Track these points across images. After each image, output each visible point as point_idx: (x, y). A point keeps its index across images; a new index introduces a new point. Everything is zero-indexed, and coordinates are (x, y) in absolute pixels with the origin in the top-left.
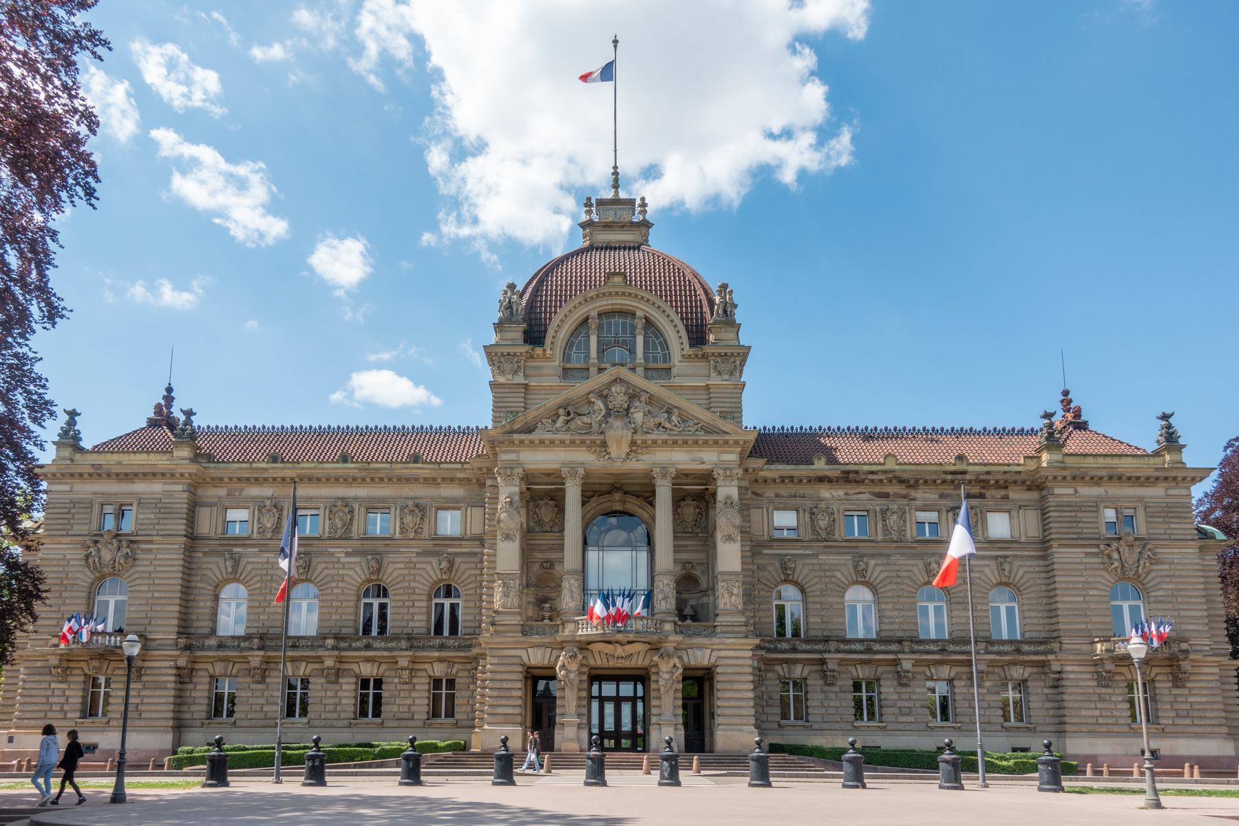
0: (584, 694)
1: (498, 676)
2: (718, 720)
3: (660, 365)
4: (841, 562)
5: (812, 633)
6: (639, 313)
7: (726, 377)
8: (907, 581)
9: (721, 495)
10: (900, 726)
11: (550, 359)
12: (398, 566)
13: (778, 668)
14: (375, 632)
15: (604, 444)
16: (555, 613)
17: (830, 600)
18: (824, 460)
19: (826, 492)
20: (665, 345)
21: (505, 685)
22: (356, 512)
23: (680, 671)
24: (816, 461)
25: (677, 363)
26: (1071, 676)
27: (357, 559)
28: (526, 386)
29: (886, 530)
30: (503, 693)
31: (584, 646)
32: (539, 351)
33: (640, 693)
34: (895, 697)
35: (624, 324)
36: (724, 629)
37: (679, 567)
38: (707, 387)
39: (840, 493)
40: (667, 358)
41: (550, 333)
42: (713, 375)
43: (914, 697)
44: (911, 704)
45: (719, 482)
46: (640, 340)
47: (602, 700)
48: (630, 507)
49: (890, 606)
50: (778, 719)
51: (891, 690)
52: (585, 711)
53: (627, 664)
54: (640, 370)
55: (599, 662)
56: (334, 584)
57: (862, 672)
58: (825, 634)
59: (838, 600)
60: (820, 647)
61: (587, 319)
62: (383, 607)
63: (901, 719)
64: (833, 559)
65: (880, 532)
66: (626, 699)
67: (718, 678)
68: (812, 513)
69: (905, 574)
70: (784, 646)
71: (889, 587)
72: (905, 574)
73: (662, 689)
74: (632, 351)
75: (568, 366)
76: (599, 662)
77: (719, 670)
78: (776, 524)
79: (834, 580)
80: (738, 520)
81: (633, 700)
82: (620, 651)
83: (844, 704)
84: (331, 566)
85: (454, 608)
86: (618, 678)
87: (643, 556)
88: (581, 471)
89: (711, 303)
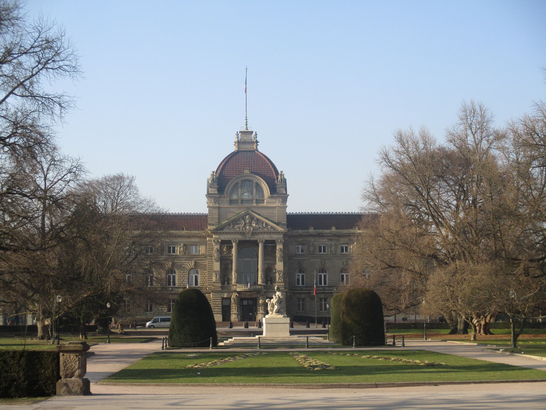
3: (261, 198)
6: (254, 181)
11: (227, 197)
13: (297, 295)
16: (229, 280)
18: (312, 228)
19: (312, 239)
20: (262, 191)
28: (219, 208)
29: (331, 251)
31: (238, 292)
32: (223, 196)
35: (249, 184)
37: (266, 266)
40: (263, 196)
41: (226, 189)
46: (254, 190)
54: (254, 201)
55: (243, 296)
57: (322, 296)
60: (309, 289)
61: (238, 183)
70: (299, 288)
74: (252, 194)
82: (248, 294)
89: (278, 178)
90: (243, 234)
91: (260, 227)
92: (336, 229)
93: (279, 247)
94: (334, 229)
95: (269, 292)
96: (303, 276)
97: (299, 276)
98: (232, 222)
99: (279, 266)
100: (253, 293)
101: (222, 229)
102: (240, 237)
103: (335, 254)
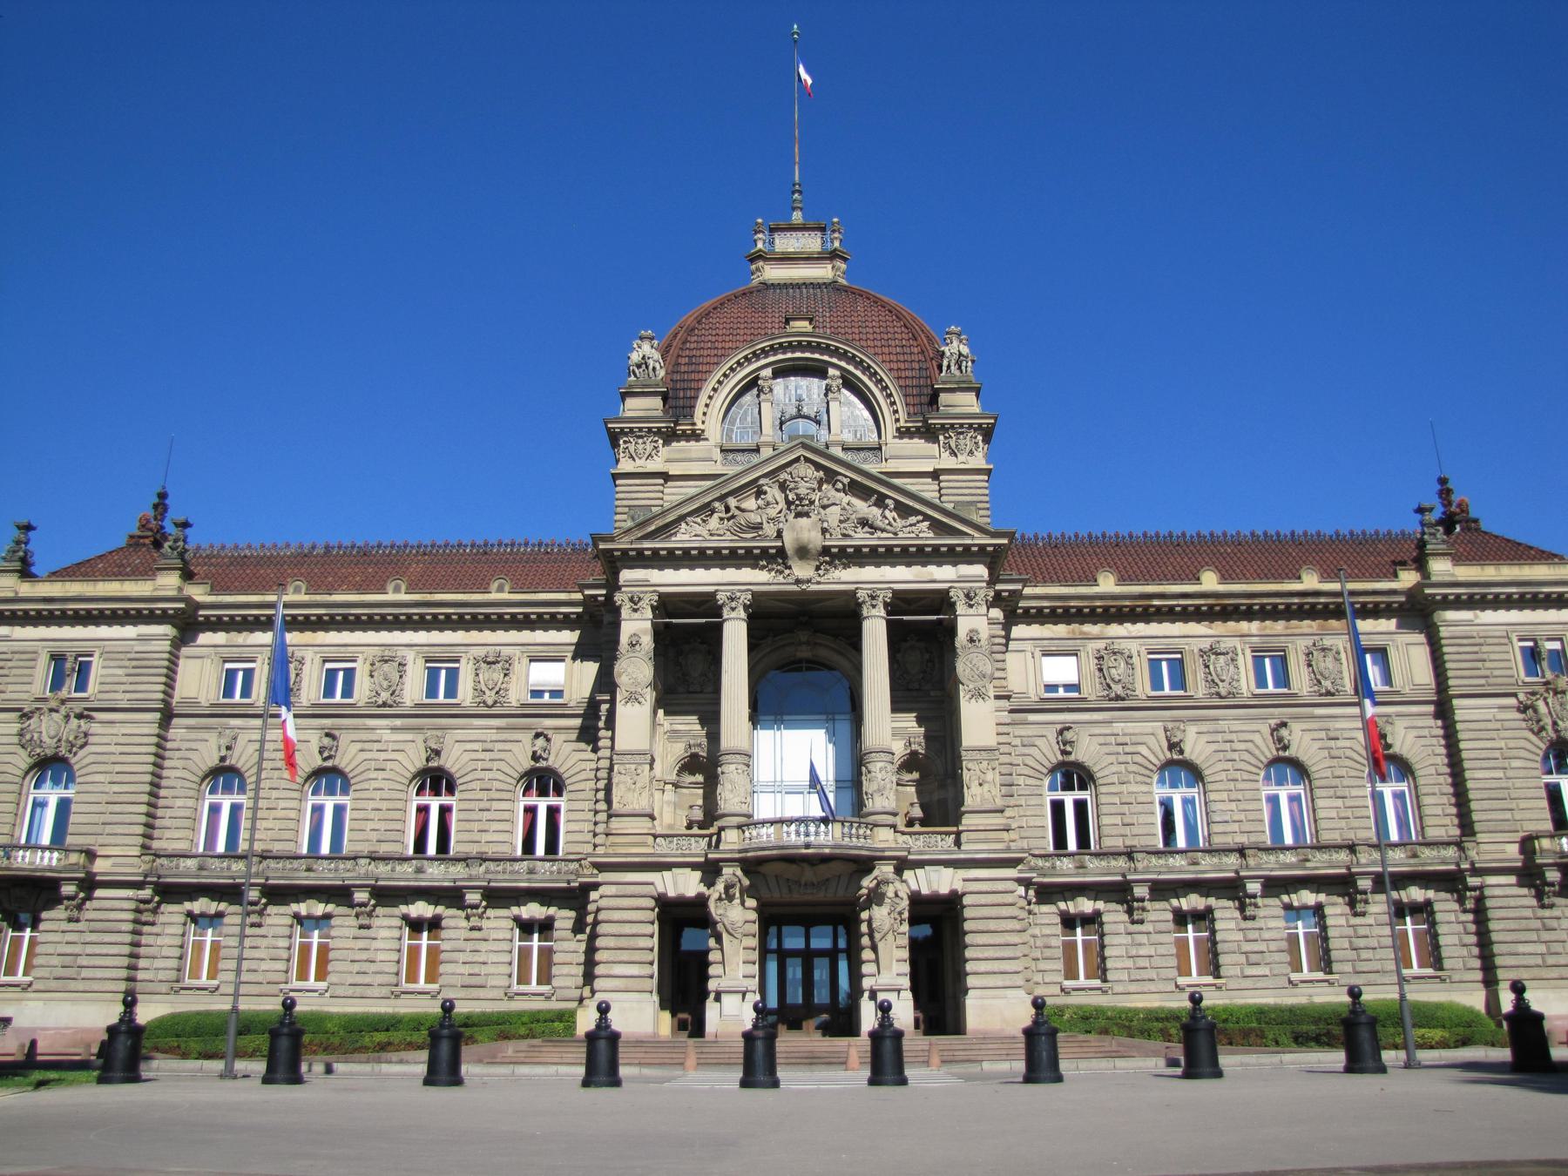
0: (754, 942)
1: (616, 915)
2: (971, 981)
4: (1148, 734)
5: (1108, 843)
6: (831, 372)
7: (961, 458)
8: (1246, 756)
9: (964, 626)
10: (1248, 983)
12: (469, 746)
14: (432, 848)
15: (781, 552)
17: (1134, 788)
21: (628, 929)
22: (409, 668)
23: (905, 903)
24: (1101, 579)
25: (890, 439)
26: (1497, 892)
27: (409, 736)
28: (666, 477)
30: (623, 942)
33: (842, 944)
34: (1240, 936)
36: (973, 835)
38: (935, 475)
39: (1140, 628)
41: (703, 399)
42: (946, 455)
43: (1266, 935)
44: (1262, 947)
45: (961, 608)
47: (783, 955)
48: (823, 653)
49: (1224, 796)
50: (1060, 978)
51: (1232, 925)
52: (755, 969)
53: (821, 896)
55: (776, 894)
56: (373, 775)
58: (1128, 843)
59: (1144, 788)
62: (445, 811)
63: (1250, 971)
64: (1131, 727)
65: (1202, 685)
66: (821, 953)
67: (967, 913)
68: (1100, 658)
69: (1242, 746)
71: (1220, 766)
72: (1242, 746)
73: (877, 936)
75: (728, 446)
76: (776, 895)
77: (966, 900)
78: (1050, 678)
79: (1138, 759)
80: (988, 668)
81: (832, 955)
82: (809, 874)
83: (1162, 950)
84: (367, 746)
85: (553, 812)
86: (808, 920)
87: (844, 727)
88: (746, 598)
90: (775, 557)
91: (864, 523)
92: (1224, 578)
93: (974, 622)
94: (1210, 581)
95: (921, 864)
96: (1080, 807)
97: (1058, 807)
98: (722, 498)
99: (978, 722)
100: (835, 867)
101: (666, 530)
102: (758, 578)
103: (1231, 694)
